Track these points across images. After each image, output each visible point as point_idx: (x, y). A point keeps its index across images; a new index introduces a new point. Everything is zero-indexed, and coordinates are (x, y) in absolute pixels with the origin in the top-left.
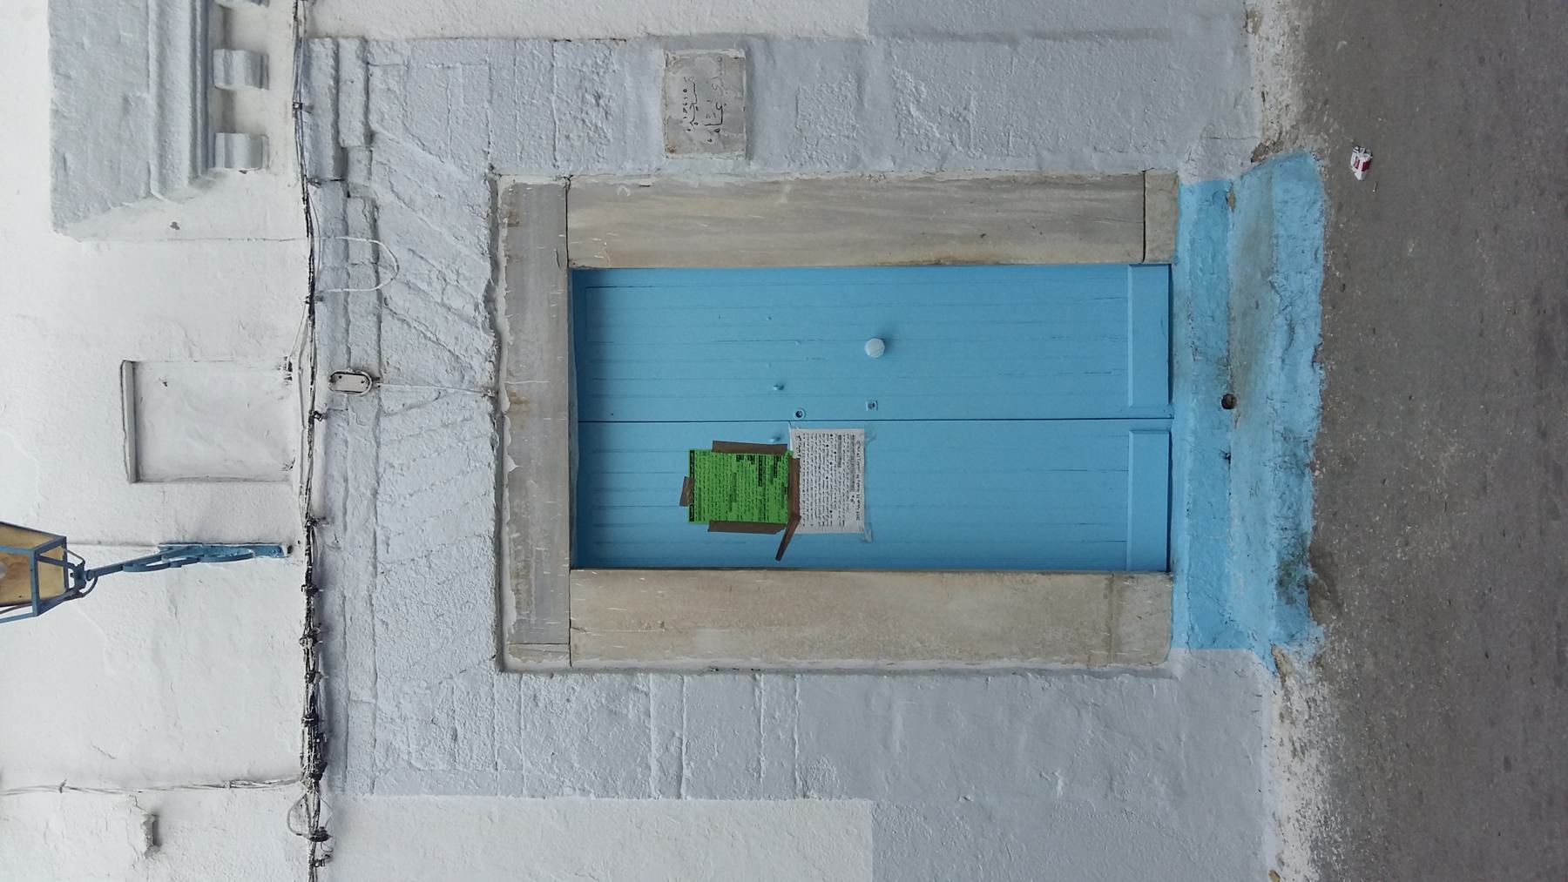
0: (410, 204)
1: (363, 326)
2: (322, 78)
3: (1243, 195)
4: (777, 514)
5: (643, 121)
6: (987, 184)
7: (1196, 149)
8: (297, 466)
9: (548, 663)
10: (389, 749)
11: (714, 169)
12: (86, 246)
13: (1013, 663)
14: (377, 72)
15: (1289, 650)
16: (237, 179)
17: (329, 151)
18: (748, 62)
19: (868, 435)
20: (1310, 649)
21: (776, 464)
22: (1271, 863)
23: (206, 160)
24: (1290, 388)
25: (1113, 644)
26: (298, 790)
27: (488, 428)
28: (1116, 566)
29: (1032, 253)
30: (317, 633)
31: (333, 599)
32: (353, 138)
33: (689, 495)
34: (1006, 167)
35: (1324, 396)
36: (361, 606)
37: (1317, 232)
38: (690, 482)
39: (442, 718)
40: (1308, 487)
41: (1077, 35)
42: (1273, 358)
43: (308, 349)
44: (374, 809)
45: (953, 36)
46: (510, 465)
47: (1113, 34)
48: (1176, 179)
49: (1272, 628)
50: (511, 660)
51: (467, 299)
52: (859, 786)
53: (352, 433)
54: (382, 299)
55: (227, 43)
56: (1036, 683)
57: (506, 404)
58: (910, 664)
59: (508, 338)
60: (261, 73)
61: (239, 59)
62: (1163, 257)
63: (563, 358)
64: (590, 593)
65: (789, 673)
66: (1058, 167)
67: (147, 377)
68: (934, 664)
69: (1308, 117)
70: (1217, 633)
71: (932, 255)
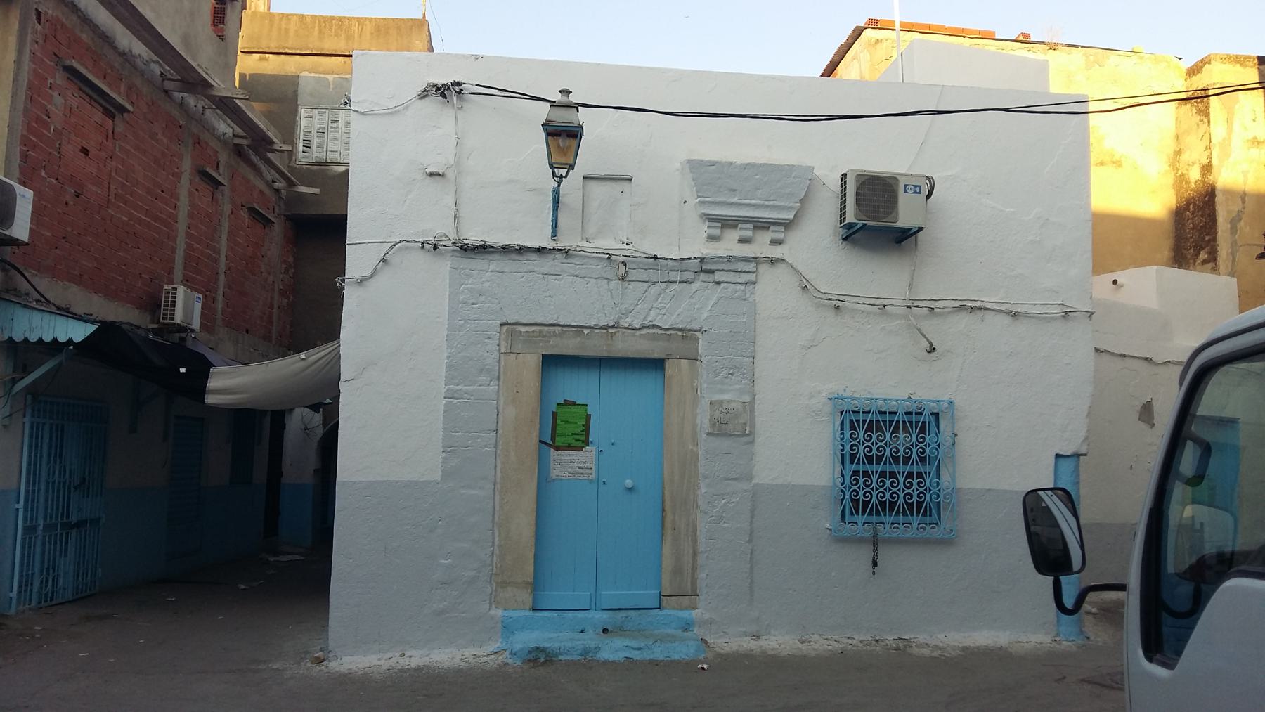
0: (691, 297)
1: (644, 275)
2: (741, 266)
3: (689, 634)
4: (560, 441)
5: (722, 392)
6: (695, 531)
7: (707, 616)
8: (585, 244)
9: (503, 343)
10: (470, 276)
11: (703, 419)
12: (678, 165)
13: (497, 542)
14: (743, 287)
15: (507, 653)
16: (703, 229)
17: (713, 267)
18: (744, 435)
19: (591, 481)
20: (510, 661)
21: (581, 441)
22: (408, 653)
23: (711, 219)
24: (614, 650)
25: (504, 585)
26: (453, 237)
27: (602, 324)
28: (535, 586)
29: (667, 550)
30: (522, 250)
31: (534, 256)
32: (717, 277)
33: (569, 403)
34: (701, 538)
35: (614, 662)
36: (530, 268)
37: (676, 657)
38: (574, 404)
39: (482, 299)
40: (576, 658)
41: (752, 568)
42: (627, 642)
43: (637, 254)
44: (444, 266)
45: (752, 517)
46: (586, 331)
47: (752, 582)
48: (695, 608)
49: (517, 647)
50: (505, 328)
51: (654, 317)
52: (447, 475)
53: (601, 268)
54: (655, 283)
55: (755, 228)
56: (489, 551)
57: (611, 331)
58: (497, 497)
59: (638, 333)
60: (742, 241)
61: (749, 233)
62: (664, 603)
63: (630, 355)
64: (533, 361)
65: (496, 446)
66: (701, 560)
67: (626, 184)
68: (497, 508)
69: (719, 655)
70: (508, 628)
71: (668, 508)
